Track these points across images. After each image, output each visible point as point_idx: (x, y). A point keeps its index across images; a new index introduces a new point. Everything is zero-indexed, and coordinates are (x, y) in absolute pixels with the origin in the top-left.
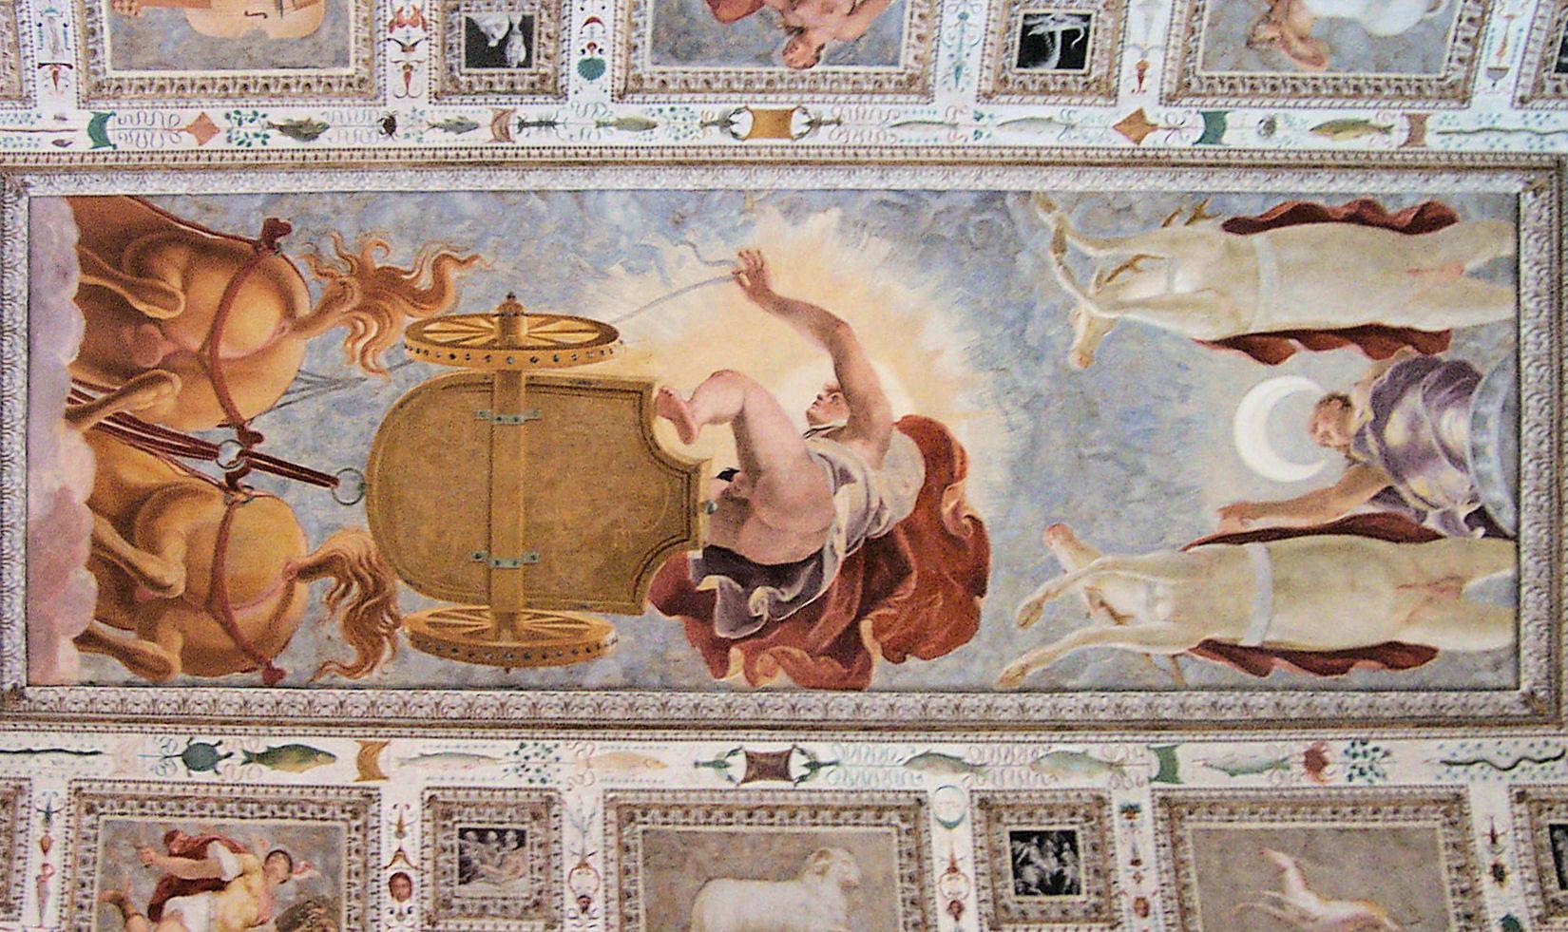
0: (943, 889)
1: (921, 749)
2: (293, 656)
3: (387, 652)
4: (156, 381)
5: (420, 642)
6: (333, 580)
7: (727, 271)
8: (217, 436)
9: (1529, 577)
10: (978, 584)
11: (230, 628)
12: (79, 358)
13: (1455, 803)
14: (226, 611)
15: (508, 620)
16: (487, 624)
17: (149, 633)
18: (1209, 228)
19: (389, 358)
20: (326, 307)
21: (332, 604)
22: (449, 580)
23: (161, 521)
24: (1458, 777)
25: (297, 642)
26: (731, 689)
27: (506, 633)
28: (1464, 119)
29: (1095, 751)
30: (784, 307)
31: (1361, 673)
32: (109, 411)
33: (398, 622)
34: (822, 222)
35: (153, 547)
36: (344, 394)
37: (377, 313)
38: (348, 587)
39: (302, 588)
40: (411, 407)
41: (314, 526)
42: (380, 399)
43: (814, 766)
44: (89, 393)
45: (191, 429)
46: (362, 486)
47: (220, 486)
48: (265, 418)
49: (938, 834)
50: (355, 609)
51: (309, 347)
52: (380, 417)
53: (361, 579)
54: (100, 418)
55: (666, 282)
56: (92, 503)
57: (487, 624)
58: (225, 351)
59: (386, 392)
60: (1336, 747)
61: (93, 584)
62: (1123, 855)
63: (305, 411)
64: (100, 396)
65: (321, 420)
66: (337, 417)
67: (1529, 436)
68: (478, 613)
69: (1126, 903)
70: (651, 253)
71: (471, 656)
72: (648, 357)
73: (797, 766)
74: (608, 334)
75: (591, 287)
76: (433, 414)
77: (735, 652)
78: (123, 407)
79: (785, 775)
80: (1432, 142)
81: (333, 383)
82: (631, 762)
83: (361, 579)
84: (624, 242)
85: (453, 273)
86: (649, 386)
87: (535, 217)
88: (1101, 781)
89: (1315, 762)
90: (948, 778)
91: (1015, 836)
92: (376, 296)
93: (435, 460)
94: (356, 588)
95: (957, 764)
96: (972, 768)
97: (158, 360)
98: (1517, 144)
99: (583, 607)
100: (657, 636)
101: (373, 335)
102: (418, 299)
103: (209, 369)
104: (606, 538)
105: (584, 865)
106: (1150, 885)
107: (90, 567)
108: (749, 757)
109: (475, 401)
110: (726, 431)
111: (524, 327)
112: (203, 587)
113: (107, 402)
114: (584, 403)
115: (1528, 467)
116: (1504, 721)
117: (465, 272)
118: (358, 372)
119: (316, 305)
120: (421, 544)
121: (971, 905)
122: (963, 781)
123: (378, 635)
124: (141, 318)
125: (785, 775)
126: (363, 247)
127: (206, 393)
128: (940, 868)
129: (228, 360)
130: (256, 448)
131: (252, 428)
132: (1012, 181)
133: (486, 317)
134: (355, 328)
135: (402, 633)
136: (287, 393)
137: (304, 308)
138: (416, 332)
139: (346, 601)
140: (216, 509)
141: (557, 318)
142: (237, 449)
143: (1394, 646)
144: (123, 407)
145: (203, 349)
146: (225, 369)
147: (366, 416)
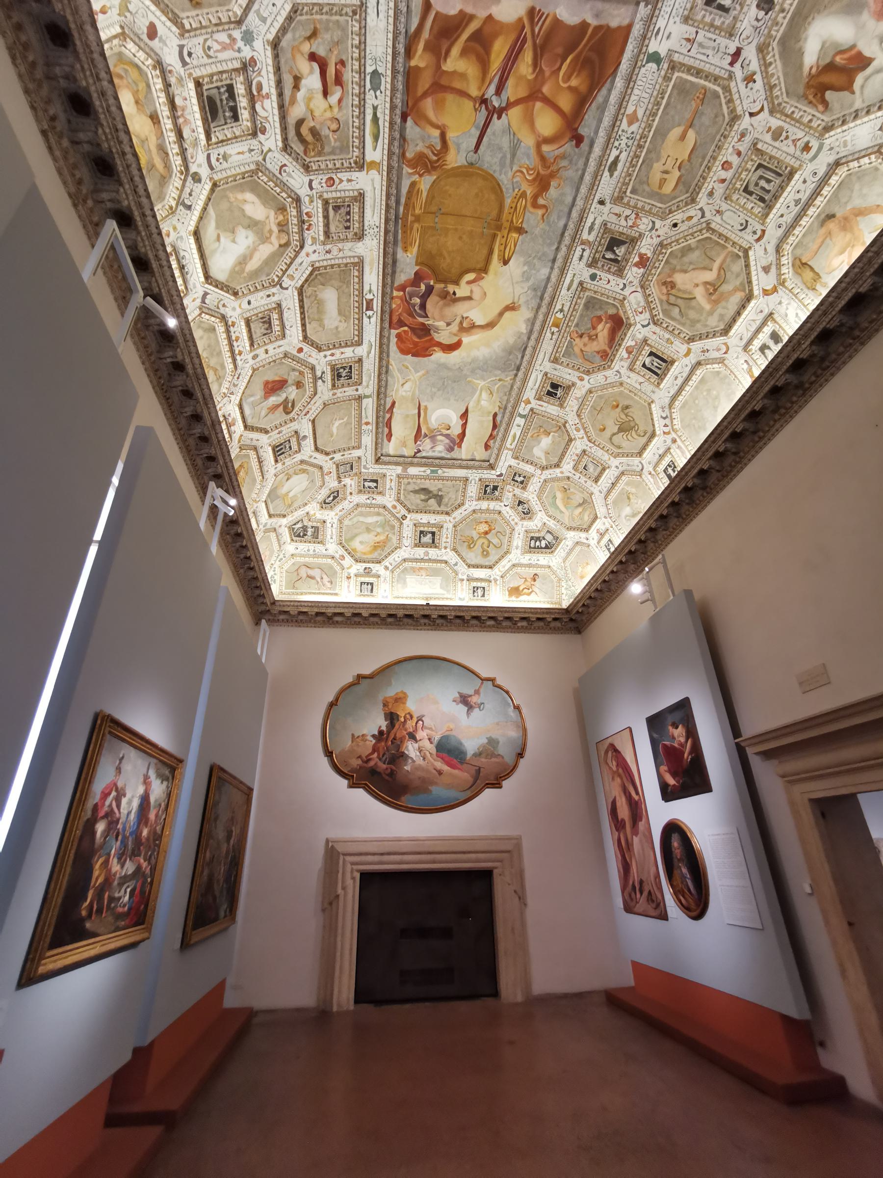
0: (337, 352)
1: (373, 344)
2: (412, 127)
3: (410, 171)
4: (535, 64)
5: (413, 184)
6: (438, 148)
7: (516, 300)
8: (504, 96)
9: (406, 459)
10: (414, 355)
11: (425, 95)
12: (558, 19)
13: (359, 447)
14: (432, 93)
15: (418, 219)
16: (417, 211)
17: (428, 47)
18: (497, 410)
19: (517, 182)
20: (542, 158)
21: (431, 147)
22: (433, 197)
23: (474, 58)
24: (363, 447)
25: (417, 129)
26: (392, 291)
27: (413, 218)
28: (509, 457)
29: (372, 382)
30: (501, 314)
31: (386, 430)
32: (529, 36)
33: (421, 176)
34: (523, 328)
35: (464, 52)
36: (508, 161)
37: (534, 180)
38: (435, 155)
39: (436, 133)
40: (497, 188)
41: (461, 141)
42: (503, 176)
43: (369, 317)
44: (540, 23)
45: (510, 83)
46: (472, 164)
47: (483, 95)
48: (506, 122)
49: (351, 349)
50: (427, 158)
51: (529, 148)
52: (496, 175)
53: (438, 160)
54: (527, 29)
55: (517, 283)
56: (490, 18)
57: (417, 211)
58: (538, 105)
59: (505, 179)
60: (370, 427)
61: (453, 12)
62: (346, 389)
63: (505, 143)
64: (537, 30)
65: (500, 149)
66: (500, 155)
67: (437, 461)
68: (421, 208)
69: (335, 391)
70: (528, 279)
71: (406, 205)
72: (496, 274)
73: (369, 313)
74: (506, 262)
75: (522, 259)
76: (493, 197)
77: (401, 293)
78: (529, 45)
79: (367, 310)
80: (506, 451)
81: (513, 155)
82: (371, 264)
83: (438, 160)
84: (534, 272)
85: (540, 212)
86: (486, 273)
87: (550, 245)
88: (364, 383)
89: (367, 424)
90: (366, 350)
91: (351, 367)
92: (541, 180)
93: (477, 195)
94: (435, 158)
95: (369, 353)
96: (368, 356)
97: (544, 67)
98: (501, 464)
99: (419, 246)
100: (408, 270)
101: (528, 177)
102: (535, 197)
103: (534, 95)
104: (441, 255)
105: (340, 250)
106: (339, 395)
107: (461, 11)
108: (372, 300)
109: (494, 214)
110: (468, 294)
111: (515, 235)
112: (444, 81)
113: (533, 31)
114: (485, 252)
115: (430, 460)
116: (376, 454)
117: (540, 217)
118: (515, 168)
119: (544, 153)
120: (448, 188)
121: (333, 358)
122: (365, 355)
123: (416, 167)
124: (564, 59)
125: (367, 310)
126: (561, 178)
127: (522, 92)
128: (342, 350)
129: (534, 106)
130: (495, 116)
131: (504, 115)
132: (521, 374)
133: (522, 223)
134: (532, 169)
135: (416, 177)
136: (514, 134)
137: (545, 148)
138: (524, 195)
139: (431, 154)
140: (474, 92)
141: (515, 246)
142: (497, 106)
143: (391, 435)
144: (529, 45)
145: (542, 93)
146: (531, 103)
147: (498, 169)
